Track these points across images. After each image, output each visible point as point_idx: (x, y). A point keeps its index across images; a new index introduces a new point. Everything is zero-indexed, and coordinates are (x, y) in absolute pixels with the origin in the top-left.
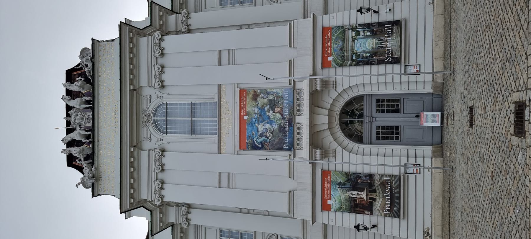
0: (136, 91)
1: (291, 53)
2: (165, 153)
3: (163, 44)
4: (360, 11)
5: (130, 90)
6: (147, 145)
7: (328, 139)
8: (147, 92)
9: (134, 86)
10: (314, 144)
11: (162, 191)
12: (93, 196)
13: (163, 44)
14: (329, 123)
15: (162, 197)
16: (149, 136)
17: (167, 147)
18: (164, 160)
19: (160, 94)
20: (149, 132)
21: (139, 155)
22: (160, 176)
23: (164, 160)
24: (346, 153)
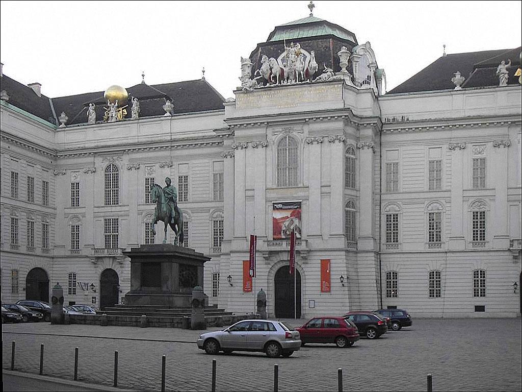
0: (305, 122)
1: (325, 237)
2: (265, 148)
3: (337, 142)
4: (342, 277)
5: (305, 119)
6: (270, 131)
7: (275, 259)
8: (306, 128)
9: (308, 121)
10: (271, 253)
11: (240, 148)
12: (234, 91)
13: (337, 142)
14: (282, 261)
15: (237, 148)
16: (276, 133)
17: (269, 148)
18: (260, 147)
19: (304, 140)
20: (278, 133)
21: (263, 127)
22: (250, 144)
23: (260, 147)
24: (268, 270)
